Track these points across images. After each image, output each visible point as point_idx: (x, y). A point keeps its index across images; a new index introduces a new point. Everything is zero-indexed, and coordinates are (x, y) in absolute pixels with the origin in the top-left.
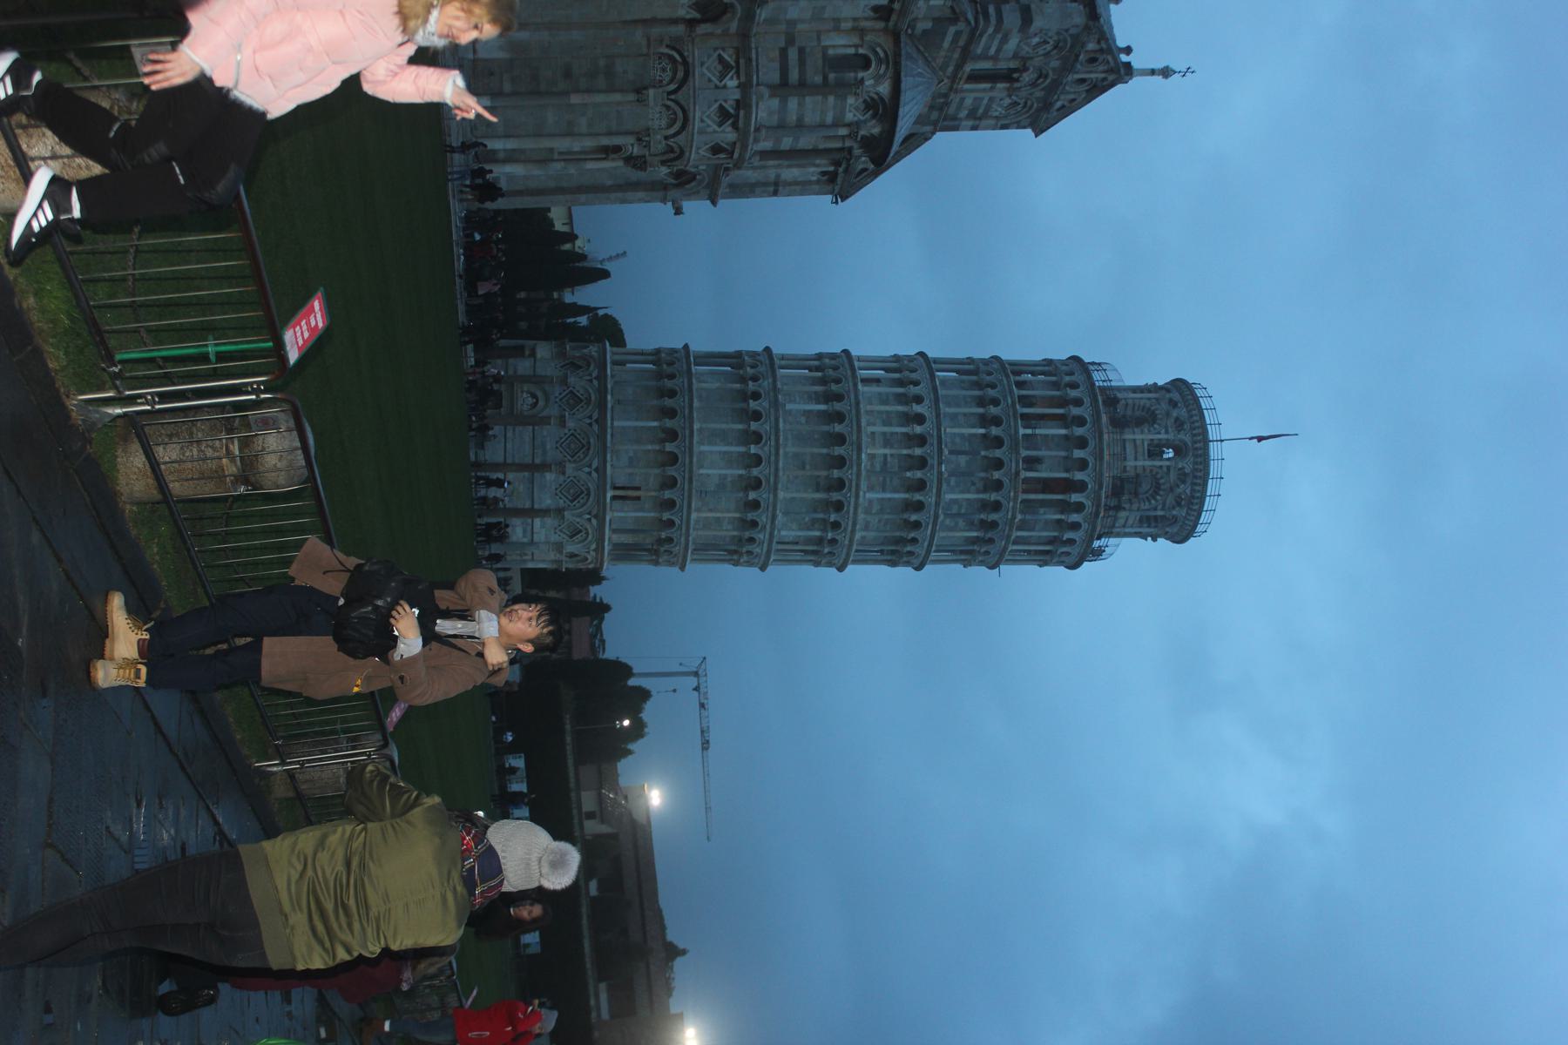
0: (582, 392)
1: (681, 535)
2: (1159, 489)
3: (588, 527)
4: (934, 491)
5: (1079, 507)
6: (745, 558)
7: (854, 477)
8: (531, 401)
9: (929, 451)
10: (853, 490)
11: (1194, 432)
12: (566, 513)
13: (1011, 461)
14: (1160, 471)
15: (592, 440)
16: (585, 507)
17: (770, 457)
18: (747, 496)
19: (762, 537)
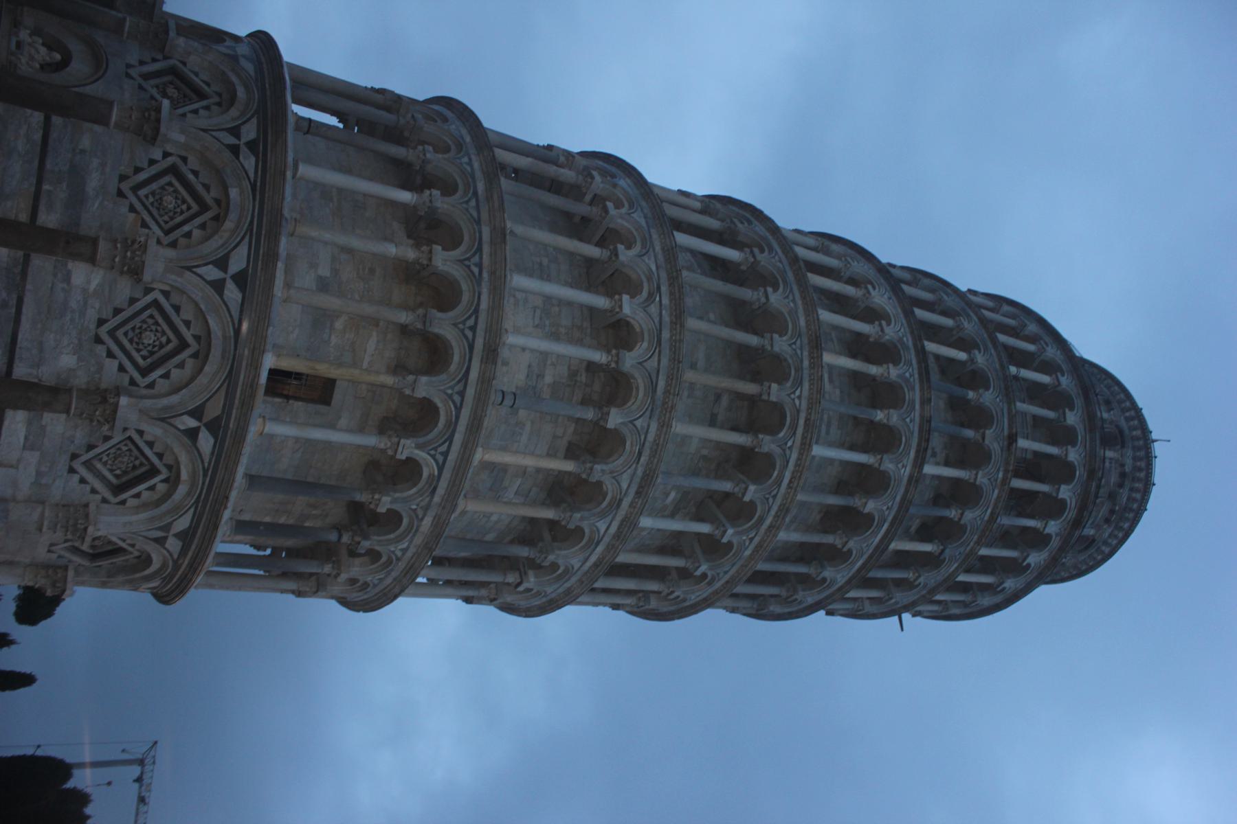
1: (426, 509)
3: (183, 458)
9: (907, 375)
12: (124, 401)
15: (234, 193)
17: (661, 334)
19: (602, 528)
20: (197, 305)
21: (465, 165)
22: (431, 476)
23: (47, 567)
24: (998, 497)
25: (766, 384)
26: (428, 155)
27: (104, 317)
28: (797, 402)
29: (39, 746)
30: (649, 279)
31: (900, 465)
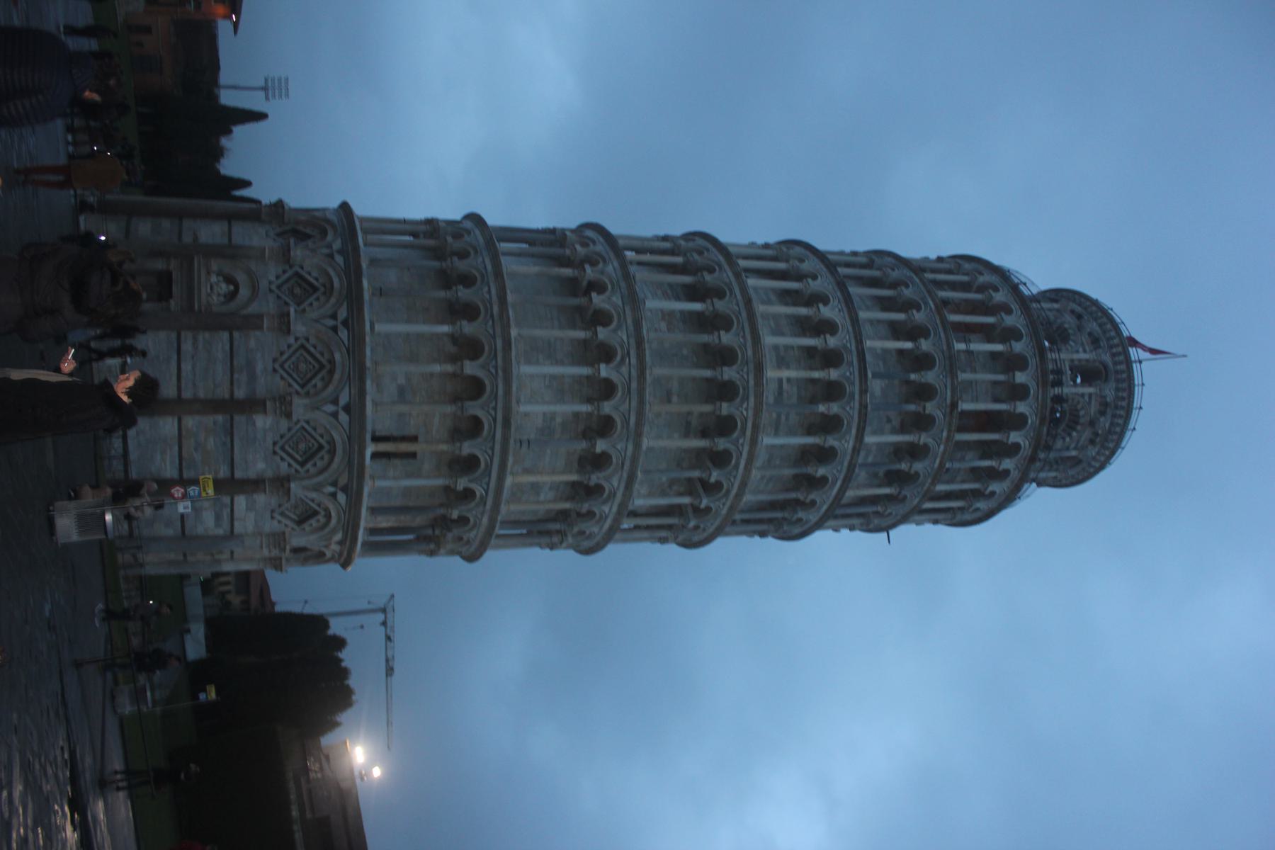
0: (315, 274)
1: (483, 514)
2: (1077, 423)
4: (854, 431)
5: (1014, 449)
6: (570, 540)
7: (751, 413)
8: (224, 288)
9: (848, 374)
10: (748, 433)
11: (1114, 350)
12: (293, 485)
13: (946, 386)
14: (1081, 400)
15: (337, 356)
16: (326, 475)
17: (630, 385)
18: (594, 446)
19: (607, 511)
20: (325, 428)
21: (485, 294)
22: (481, 495)
23: (271, 559)
24: (945, 450)
25: (718, 404)
26: (460, 294)
27: (276, 439)
28: (745, 413)
29: (306, 602)
30: (622, 347)
31: (843, 442)
